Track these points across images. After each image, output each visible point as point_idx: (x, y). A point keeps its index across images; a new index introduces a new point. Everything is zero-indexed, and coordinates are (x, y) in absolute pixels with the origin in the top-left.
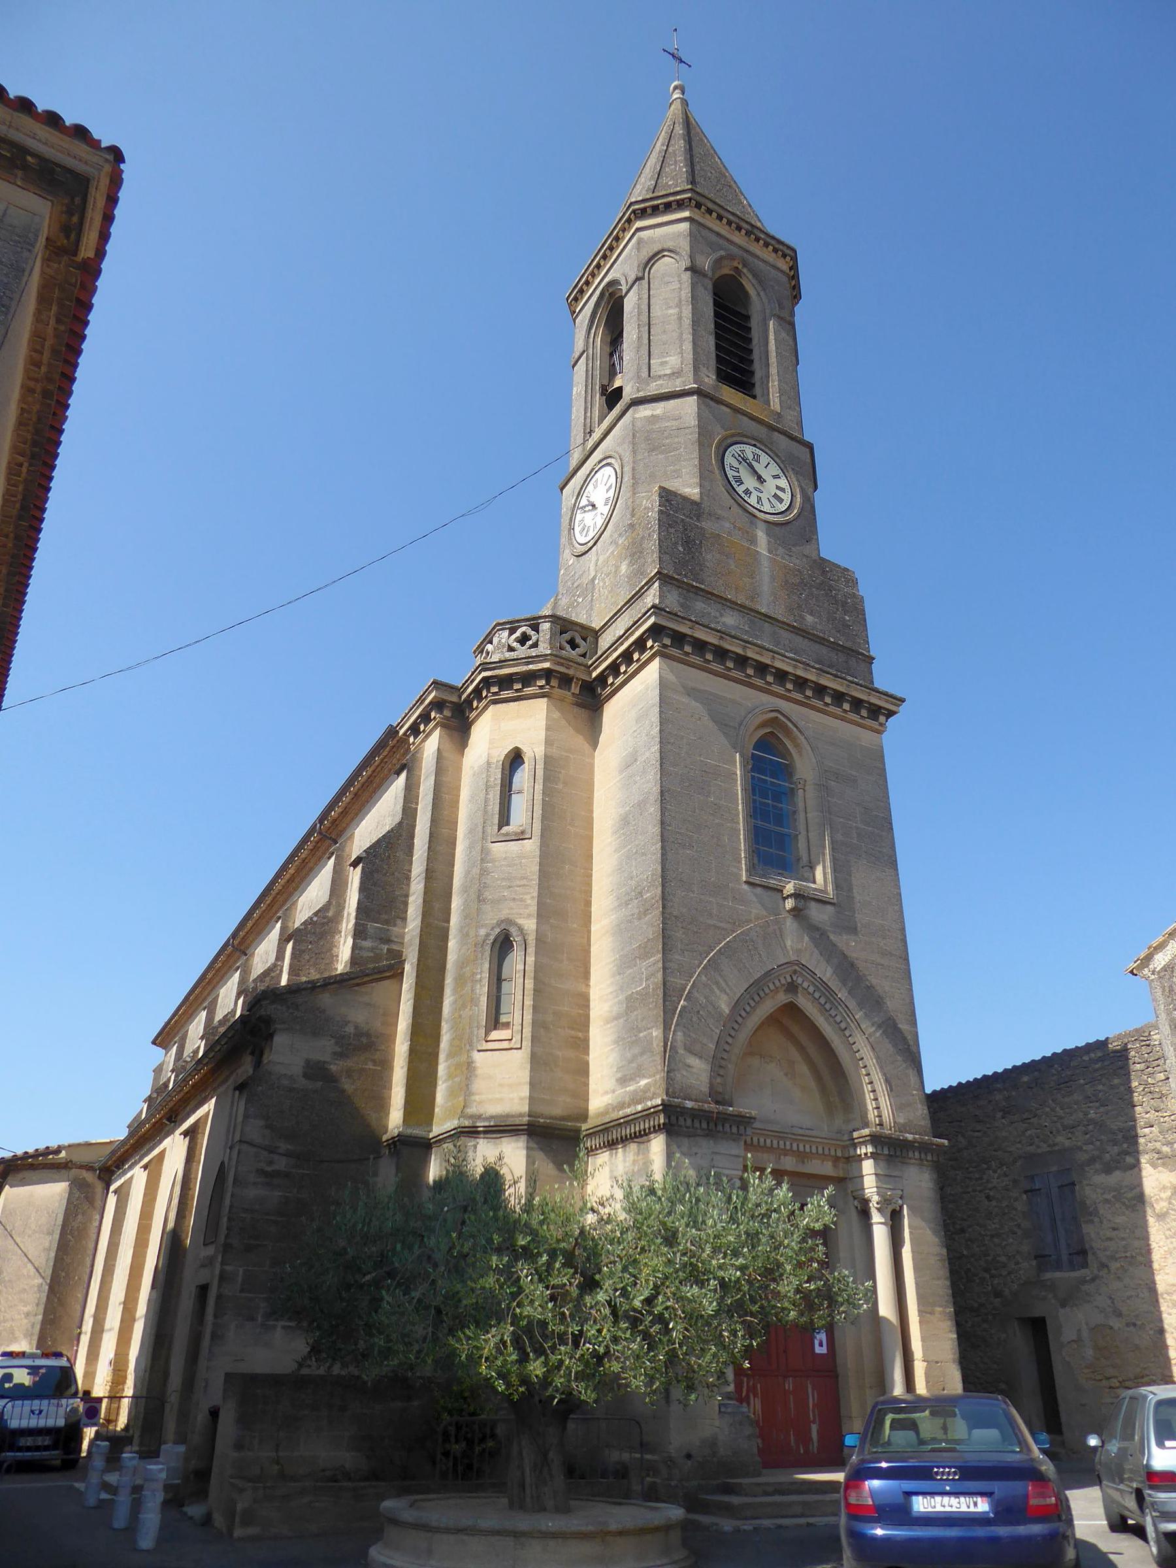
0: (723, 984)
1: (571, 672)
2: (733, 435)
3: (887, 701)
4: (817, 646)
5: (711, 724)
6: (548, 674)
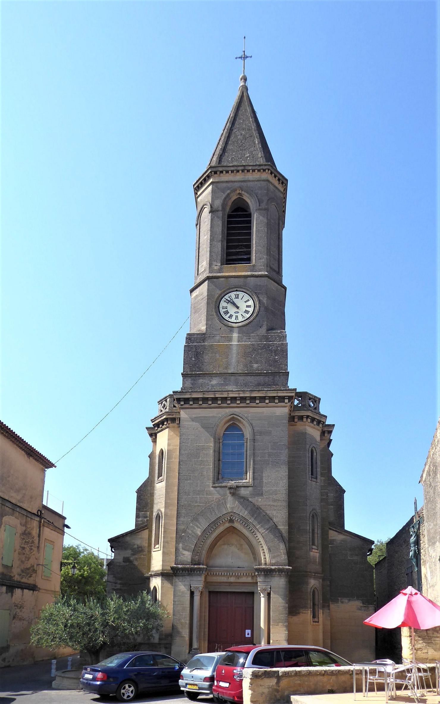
0: (199, 525)
1: (174, 416)
2: (224, 292)
3: (287, 393)
4: (258, 377)
5: (202, 430)
6: (166, 419)
